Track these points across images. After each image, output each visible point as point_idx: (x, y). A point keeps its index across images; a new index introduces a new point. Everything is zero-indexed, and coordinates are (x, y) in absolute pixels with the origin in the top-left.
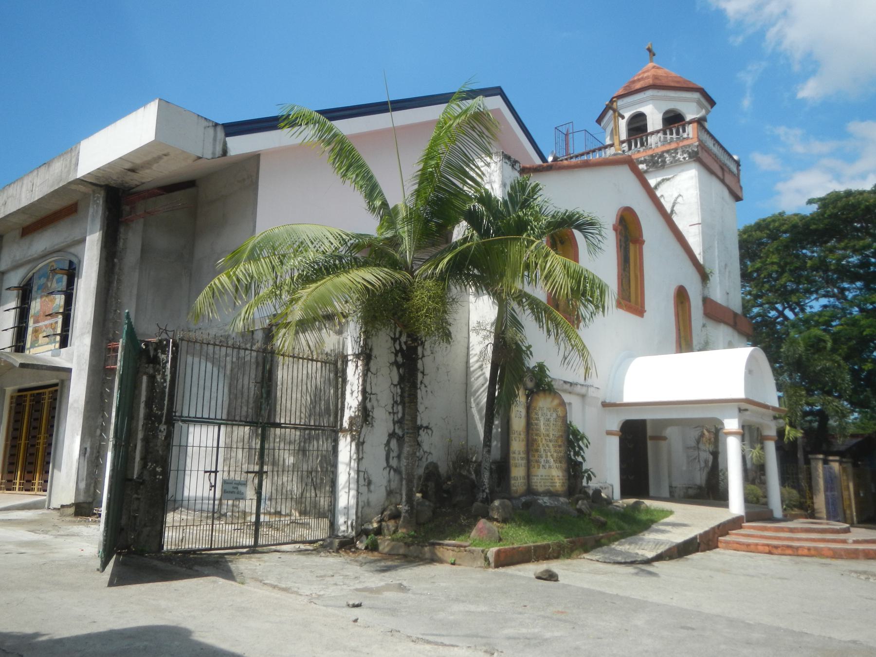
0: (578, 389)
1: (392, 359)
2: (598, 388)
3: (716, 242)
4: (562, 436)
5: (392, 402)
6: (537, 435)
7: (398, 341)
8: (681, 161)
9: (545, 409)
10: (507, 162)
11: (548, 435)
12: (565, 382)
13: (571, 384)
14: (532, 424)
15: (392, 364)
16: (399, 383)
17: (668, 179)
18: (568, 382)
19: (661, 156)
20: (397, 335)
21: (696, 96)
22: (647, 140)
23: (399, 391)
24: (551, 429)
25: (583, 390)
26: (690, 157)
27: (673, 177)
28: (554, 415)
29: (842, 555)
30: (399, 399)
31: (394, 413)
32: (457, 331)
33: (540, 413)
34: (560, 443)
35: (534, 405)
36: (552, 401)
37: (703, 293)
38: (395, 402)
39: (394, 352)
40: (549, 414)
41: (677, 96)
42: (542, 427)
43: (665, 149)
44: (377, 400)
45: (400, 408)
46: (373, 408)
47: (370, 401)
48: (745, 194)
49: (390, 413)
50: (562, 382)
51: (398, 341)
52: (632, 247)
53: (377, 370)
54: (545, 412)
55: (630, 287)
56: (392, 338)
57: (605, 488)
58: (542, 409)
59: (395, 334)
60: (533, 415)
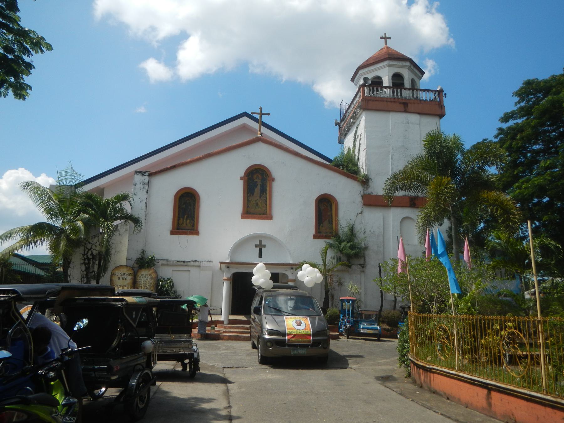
0: (192, 263)
1: (82, 261)
2: (210, 261)
3: (391, 155)
4: (153, 286)
5: (81, 277)
6: (139, 286)
7: (86, 255)
9: (145, 275)
10: (139, 174)
11: (146, 286)
12: (178, 261)
13: (184, 262)
14: (137, 282)
15: (82, 264)
16: (85, 270)
17: (359, 125)
18: (181, 261)
20: (86, 253)
21: (386, 63)
23: (85, 273)
24: (147, 283)
25: (197, 264)
27: (360, 123)
28: (150, 277)
29: (196, 336)
30: (85, 276)
31: (82, 281)
32: (122, 247)
33: (142, 277)
34: (152, 289)
35: (139, 273)
36: (149, 271)
37: (363, 192)
38: (83, 277)
39: (83, 259)
40: (147, 277)
41: (364, 71)
42: (143, 283)
44: (73, 277)
45: (85, 279)
46: (71, 280)
47: (69, 277)
49: (79, 281)
50: (176, 262)
51: (86, 255)
53: (74, 267)
54: (145, 276)
55: (266, 205)
56: (83, 254)
57: (214, 309)
58: (143, 275)
59: (84, 253)
60: (138, 278)
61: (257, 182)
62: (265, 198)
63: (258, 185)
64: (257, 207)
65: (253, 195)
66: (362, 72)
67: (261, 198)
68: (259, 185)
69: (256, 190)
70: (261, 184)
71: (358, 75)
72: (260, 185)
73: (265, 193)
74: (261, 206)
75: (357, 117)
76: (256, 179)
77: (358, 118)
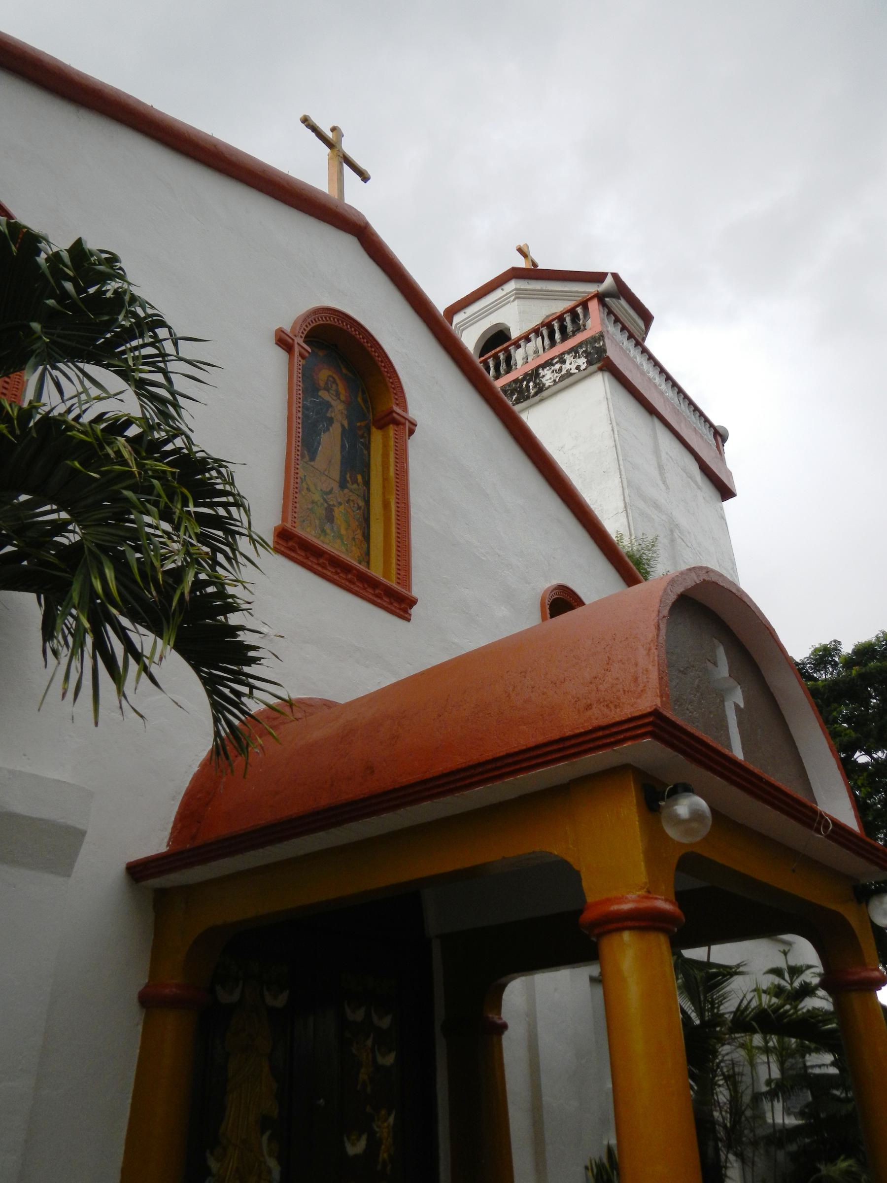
8: (572, 374)
19: (534, 375)
22: (509, 358)
26: (590, 363)
43: (541, 361)
48: (738, 484)
52: (377, 437)
55: (367, 537)
61: (328, 405)
62: (362, 503)
63: (331, 421)
64: (327, 527)
65: (312, 459)
66: (522, 287)
67: (346, 491)
68: (336, 430)
69: (324, 438)
70: (346, 424)
71: (498, 294)
72: (343, 426)
73: (359, 477)
74: (343, 532)
75: (545, 394)
76: (327, 389)
77: (541, 400)
